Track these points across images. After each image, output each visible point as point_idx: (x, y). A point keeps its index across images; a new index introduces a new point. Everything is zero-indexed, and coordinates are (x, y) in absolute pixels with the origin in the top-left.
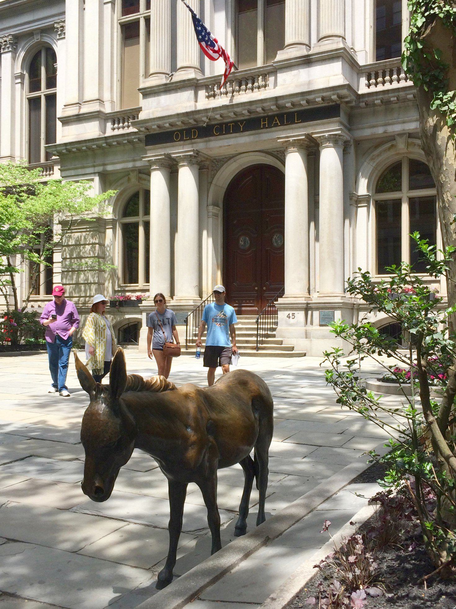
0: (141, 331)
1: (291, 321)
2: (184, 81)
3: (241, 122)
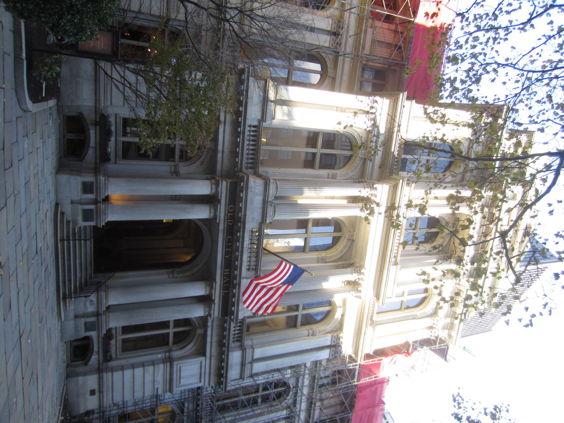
0: (77, 177)
1: (88, 303)
2: (266, 217)
3: (231, 257)
